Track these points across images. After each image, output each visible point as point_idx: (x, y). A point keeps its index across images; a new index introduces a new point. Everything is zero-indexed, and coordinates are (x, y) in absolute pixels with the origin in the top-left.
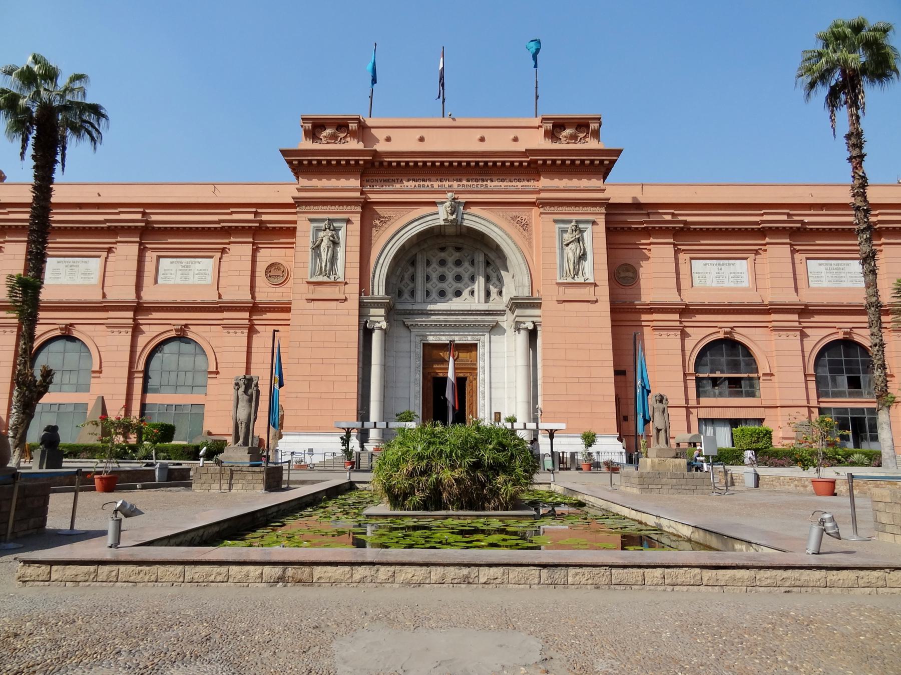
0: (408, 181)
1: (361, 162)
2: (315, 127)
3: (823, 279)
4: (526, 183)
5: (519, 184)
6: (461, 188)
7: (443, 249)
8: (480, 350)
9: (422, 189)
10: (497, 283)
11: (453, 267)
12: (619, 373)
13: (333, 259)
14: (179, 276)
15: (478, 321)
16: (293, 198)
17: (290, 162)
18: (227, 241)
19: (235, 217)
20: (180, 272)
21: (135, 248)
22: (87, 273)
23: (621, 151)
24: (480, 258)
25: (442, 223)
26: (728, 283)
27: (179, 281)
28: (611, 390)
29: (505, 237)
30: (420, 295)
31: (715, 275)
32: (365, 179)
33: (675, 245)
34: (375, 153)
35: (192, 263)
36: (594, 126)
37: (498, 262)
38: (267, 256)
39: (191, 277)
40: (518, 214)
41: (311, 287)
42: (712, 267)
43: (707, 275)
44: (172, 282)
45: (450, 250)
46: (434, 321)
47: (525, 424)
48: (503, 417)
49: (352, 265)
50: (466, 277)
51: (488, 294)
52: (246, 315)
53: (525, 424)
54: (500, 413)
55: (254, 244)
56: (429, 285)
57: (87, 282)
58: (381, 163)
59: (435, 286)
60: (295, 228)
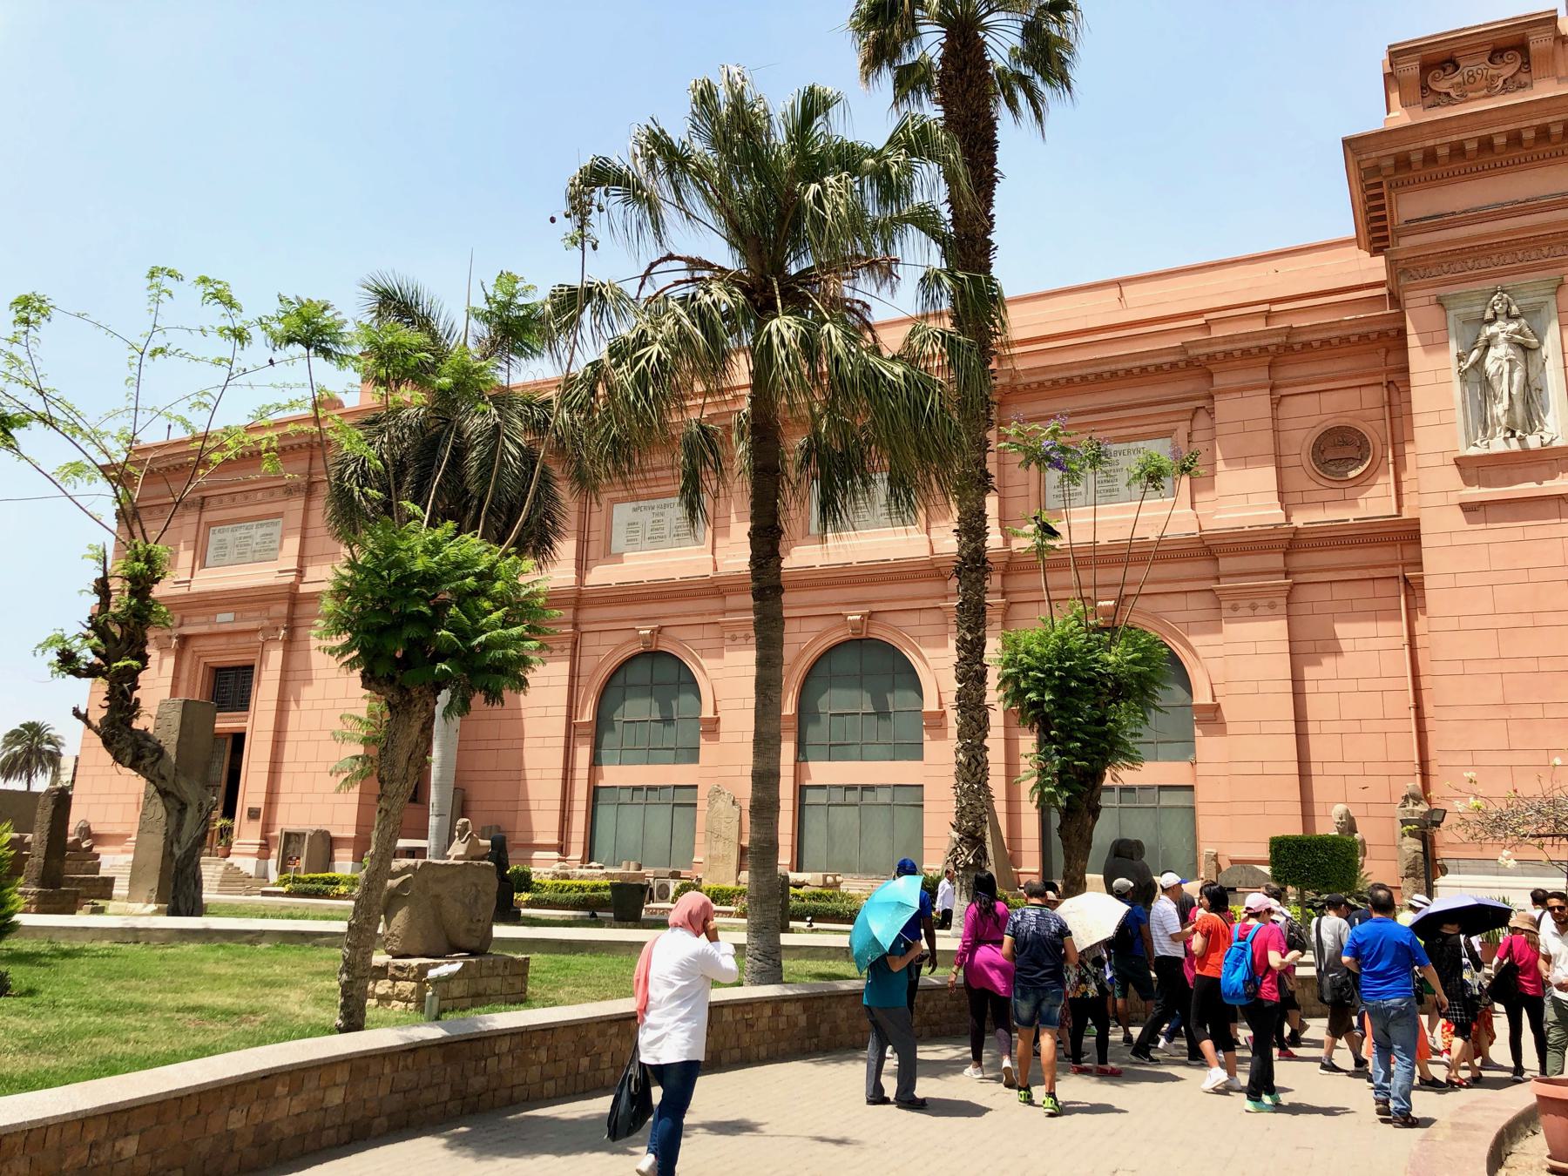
2: (1425, 67)
38: (1313, 412)
52: (1276, 561)
55: (1273, 388)
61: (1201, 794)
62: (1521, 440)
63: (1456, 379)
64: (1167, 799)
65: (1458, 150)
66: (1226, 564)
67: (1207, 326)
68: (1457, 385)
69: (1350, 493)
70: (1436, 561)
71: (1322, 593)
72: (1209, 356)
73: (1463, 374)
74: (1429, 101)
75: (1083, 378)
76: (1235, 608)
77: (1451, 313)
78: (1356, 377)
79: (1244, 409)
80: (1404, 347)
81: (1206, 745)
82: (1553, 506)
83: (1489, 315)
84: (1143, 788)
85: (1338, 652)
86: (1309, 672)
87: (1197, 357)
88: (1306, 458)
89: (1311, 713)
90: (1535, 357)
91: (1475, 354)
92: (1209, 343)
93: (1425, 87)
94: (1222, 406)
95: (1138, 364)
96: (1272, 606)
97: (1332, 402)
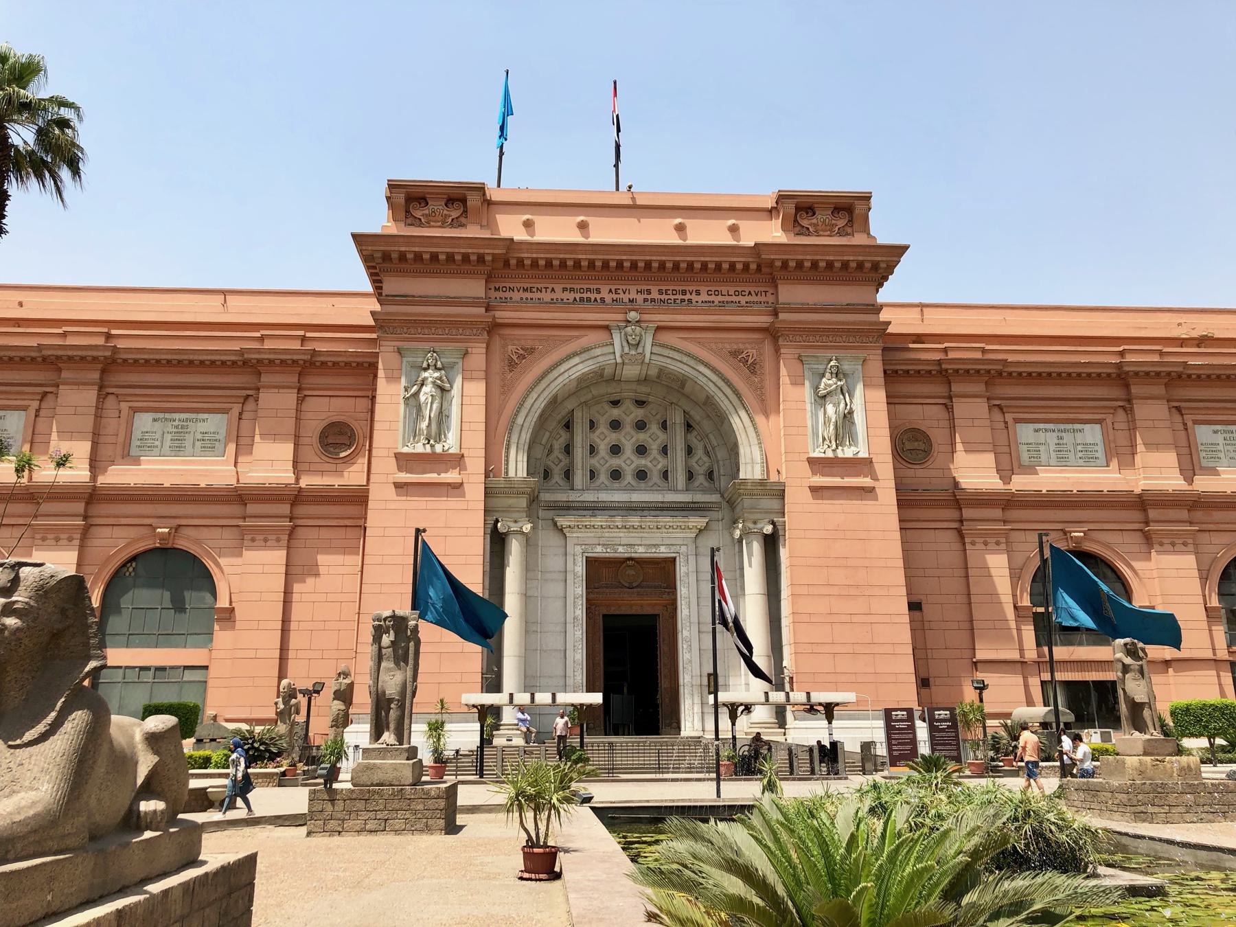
0: (564, 290)
2: (409, 198)
3: (1222, 455)
4: (753, 298)
5: (743, 300)
7: (615, 403)
10: (706, 459)
11: (633, 432)
12: (914, 606)
13: (442, 418)
16: (373, 313)
19: (268, 345)
20: (168, 437)
21: (91, 395)
23: (906, 248)
25: (619, 360)
28: (906, 636)
29: (720, 383)
30: (579, 478)
31: (1052, 447)
32: (492, 286)
36: (859, 208)
37: (707, 425)
38: (323, 410)
40: (741, 346)
42: (1048, 434)
43: (1042, 448)
45: (628, 404)
47: (766, 693)
49: (473, 426)
50: (654, 448)
51: (690, 476)
52: (285, 509)
53: (766, 693)
55: (299, 390)
56: (594, 461)
58: (520, 262)
59: (605, 462)
61: (212, 672)
62: (432, 446)
63: (402, 401)
64: (189, 676)
65: (418, 257)
66: (252, 508)
67: (262, 339)
68: (402, 406)
69: (340, 467)
70: (374, 518)
71: (313, 533)
72: (258, 360)
73: (406, 399)
74: (409, 221)
75: (169, 361)
76: (253, 540)
77: (405, 360)
78: (354, 390)
79: (277, 400)
80: (375, 376)
81: (222, 637)
82: (444, 489)
83: (425, 365)
84: (172, 668)
85: (317, 575)
86: (297, 587)
87: (250, 360)
88: (315, 440)
89: (295, 616)
90: (448, 395)
91: (415, 388)
92: (258, 351)
93: (407, 212)
94: (263, 395)
95: (209, 358)
96: (278, 540)
97: (337, 403)
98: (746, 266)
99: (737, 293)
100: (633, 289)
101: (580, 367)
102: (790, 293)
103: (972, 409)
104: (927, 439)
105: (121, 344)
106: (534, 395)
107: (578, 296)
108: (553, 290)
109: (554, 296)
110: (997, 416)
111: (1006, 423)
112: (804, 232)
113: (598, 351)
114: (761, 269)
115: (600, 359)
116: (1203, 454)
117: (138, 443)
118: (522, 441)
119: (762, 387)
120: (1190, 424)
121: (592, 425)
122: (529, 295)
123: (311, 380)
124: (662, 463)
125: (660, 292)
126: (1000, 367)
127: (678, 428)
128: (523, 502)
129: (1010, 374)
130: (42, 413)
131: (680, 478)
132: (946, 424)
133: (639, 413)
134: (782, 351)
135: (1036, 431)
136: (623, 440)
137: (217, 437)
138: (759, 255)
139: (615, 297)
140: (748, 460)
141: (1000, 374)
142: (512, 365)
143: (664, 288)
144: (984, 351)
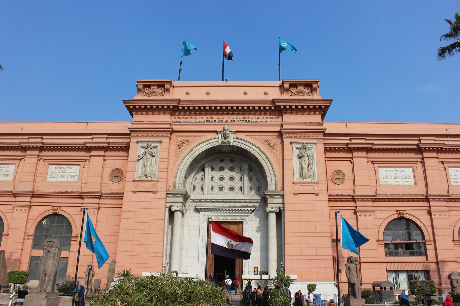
0: (200, 118)
1: (171, 107)
4: (274, 120)
5: (270, 120)
6: (233, 123)
7: (222, 161)
8: (245, 226)
9: (208, 123)
10: (257, 182)
14: (59, 176)
15: (244, 207)
17: (128, 107)
18: (89, 154)
19: (95, 140)
20: (59, 174)
22: (6, 174)
23: (332, 101)
24: (245, 167)
26: (401, 183)
27: (59, 180)
31: (393, 177)
33: (367, 158)
34: (179, 101)
35: (67, 168)
38: (112, 164)
39: (66, 177)
40: (269, 138)
41: (136, 183)
42: (391, 172)
43: (389, 178)
44: (55, 180)
46: (215, 206)
48: (259, 270)
52: (97, 201)
54: (257, 267)
56: (213, 183)
57: (6, 179)
58: (183, 107)
59: (217, 183)
60: (129, 147)
66: (86, 200)
72: (91, 146)
74: (144, 94)
77: (139, 145)
88: (109, 175)
98: (270, 107)
99: (267, 118)
100: (227, 117)
101: (206, 146)
102: (288, 118)
103: (361, 162)
104: (344, 175)
105: (45, 141)
106: (187, 158)
107: (205, 120)
108: (196, 118)
109: (196, 120)
110: (370, 164)
111: (374, 168)
112: (293, 94)
113: (213, 141)
114: (276, 109)
115: (213, 144)
116: (452, 180)
117: (50, 176)
118: (181, 176)
119: (277, 154)
120: (447, 168)
121: (213, 169)
122: (187, 120)
123: (109, 153)
124: (240, 184)
125: (237, 118)
126: (371, 146)
127: (246, 171)
128: (181, 200)
129: (376, 148)
130: (20, 166)
131: (246, 189)
132: (351, 168)
133: (231, 164)
134: (284, 140)
135: (387, 171)
136: (224, 175)
137: (76, 174)
138: (275, 104)
139: (220, 120)
140: (271, 183)
141: (371, 148)
142: (179, 146)
143: (239, 116)
144: (365, 140)
